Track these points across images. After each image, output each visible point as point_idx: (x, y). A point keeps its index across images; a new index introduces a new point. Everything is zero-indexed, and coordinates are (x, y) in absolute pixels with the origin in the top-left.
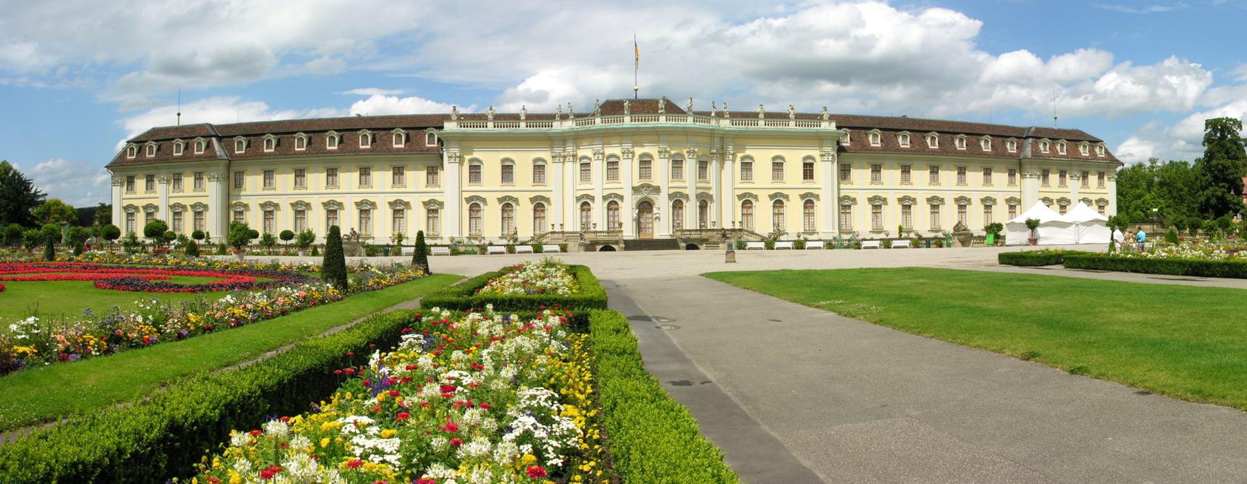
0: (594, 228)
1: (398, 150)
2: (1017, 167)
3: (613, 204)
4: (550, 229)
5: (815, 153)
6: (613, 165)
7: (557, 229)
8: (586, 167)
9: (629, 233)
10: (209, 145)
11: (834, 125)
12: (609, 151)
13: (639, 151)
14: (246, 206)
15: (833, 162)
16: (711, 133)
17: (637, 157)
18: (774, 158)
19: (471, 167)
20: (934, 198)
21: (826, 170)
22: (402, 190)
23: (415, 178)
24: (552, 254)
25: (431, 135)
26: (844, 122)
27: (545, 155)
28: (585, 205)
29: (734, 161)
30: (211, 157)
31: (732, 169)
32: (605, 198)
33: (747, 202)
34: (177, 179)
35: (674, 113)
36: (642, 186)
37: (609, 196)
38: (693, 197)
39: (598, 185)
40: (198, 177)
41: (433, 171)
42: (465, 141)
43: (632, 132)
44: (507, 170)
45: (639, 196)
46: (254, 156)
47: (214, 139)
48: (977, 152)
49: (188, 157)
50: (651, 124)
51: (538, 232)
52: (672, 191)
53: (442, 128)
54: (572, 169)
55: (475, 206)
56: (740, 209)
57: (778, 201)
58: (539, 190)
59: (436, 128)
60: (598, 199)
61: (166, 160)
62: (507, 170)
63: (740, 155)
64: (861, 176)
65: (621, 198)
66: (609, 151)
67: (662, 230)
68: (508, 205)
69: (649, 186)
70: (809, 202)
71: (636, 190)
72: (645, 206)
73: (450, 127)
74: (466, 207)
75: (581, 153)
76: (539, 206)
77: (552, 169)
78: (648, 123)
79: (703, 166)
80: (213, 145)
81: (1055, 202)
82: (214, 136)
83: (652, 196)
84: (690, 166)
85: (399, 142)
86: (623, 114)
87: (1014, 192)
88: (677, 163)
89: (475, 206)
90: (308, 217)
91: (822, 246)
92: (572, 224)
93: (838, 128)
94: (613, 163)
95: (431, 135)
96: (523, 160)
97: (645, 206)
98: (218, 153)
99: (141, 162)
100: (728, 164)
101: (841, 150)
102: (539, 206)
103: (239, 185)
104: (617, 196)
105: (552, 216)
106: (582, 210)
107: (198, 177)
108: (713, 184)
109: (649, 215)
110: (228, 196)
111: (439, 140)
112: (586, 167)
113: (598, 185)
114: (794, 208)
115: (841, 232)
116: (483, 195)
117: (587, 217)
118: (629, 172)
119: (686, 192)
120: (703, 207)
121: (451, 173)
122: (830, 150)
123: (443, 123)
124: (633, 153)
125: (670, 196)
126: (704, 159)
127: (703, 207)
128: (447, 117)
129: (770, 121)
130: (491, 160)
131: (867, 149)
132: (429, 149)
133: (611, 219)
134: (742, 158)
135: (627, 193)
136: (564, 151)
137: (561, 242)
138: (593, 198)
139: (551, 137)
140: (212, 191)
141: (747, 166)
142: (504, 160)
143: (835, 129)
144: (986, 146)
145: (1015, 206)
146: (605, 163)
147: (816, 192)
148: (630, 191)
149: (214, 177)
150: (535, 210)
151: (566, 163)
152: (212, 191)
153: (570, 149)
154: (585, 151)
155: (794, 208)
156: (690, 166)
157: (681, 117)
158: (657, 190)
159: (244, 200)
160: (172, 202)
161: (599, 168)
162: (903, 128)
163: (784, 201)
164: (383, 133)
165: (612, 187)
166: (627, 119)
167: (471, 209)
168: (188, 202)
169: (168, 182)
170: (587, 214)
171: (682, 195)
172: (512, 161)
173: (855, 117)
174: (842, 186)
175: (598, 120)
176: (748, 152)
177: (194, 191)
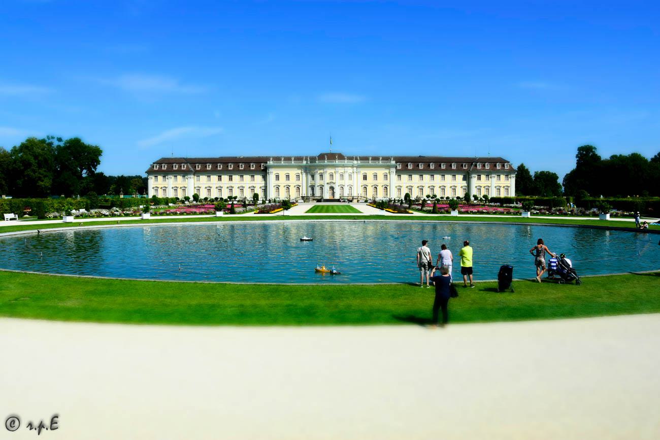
3: (322, 187)
6: (321, 176)
7: (303, 196)
8: (313, 177)
9: (327, 196)
10: (187, 167)
11: (394, 162)
21: (394, 176)
23: (259, 178)
26: (399, 160)
36: (331, 183)
44: (288, 177)
45: (329, 186)
50: (334, 163)
53: (267, 163)
61: (171, 171)
62: (288, 177)
64: (405, 177)
65: (323, 186)
67: (337, 197)
72: (332, 188)
73: (271, 163)
88: (342, 176)
93: (396, 162)
97: (332, 188)
112: (313, 177)
114: (380, 190)
116: (279, 184)
121: (271, 177)
130: (282, 173)
155: (380, 190)
156: (346, 176)
157: (343, 161)
158: (334, 183)
165: (322, 182)
168: (179, 186)
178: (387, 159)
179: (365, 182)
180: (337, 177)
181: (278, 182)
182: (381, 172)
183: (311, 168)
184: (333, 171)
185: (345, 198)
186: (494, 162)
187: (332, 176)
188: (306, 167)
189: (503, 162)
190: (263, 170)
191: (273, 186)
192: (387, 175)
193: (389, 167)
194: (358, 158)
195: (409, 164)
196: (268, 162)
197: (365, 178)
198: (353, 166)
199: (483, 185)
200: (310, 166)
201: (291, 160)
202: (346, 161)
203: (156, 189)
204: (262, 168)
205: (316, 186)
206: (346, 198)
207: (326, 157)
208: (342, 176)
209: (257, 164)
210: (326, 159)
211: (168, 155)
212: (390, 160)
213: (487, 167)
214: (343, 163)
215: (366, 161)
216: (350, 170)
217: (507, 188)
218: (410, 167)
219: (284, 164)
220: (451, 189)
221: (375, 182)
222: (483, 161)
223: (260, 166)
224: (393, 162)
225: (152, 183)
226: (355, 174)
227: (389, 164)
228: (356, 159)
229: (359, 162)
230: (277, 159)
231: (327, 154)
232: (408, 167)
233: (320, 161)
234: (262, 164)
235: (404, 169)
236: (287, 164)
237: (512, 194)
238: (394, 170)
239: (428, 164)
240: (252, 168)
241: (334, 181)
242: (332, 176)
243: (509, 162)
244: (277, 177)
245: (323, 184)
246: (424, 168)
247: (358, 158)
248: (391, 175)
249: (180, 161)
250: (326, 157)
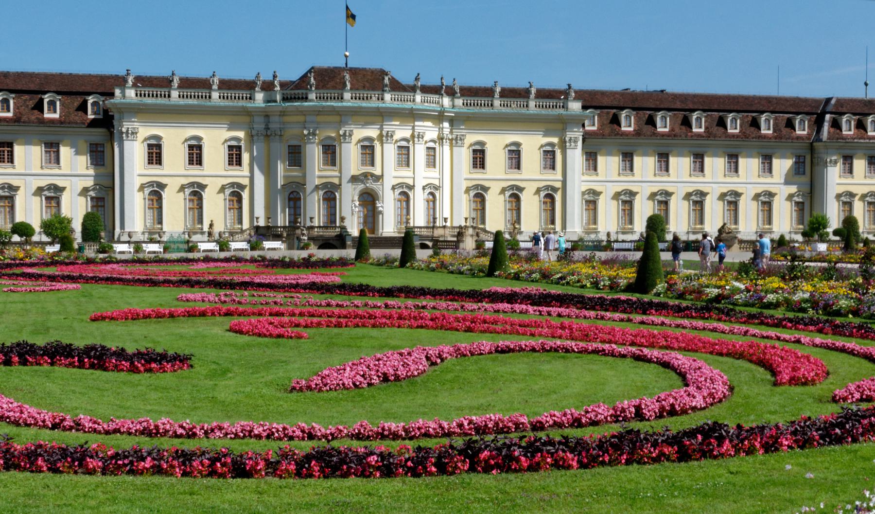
0: (311, 222)
1: (52, 121)
3: (330, 193)
24: (626, 253)
33: (479, 196)
35: (514, 97)
36: (366, 175)
43: (352, 111)
45: (361, 187)
48: (754, 136)
50: (374, 103)
53: (112, 95)
57: (515, 197)
59: (102, 94)
69: (372, 175)
72: (369, 200)
78: (470, 108)
90: (395, 211)
91: (736, 246)
106: (290, 199)
115: (588, 233)
120: (432, 200)
123: (114, 88)
127: (432, 200)
128: (120, 81)
129: (506, 101)
131: (618, 134)
139: (250, 112)
143: (581, 111)
157: (408, 95)
162: (662, 106)
166: (347, 95)
170: (295, 204)
173: (603, 93)
179: (479, 176)
180: (388, 154)
181: (155, 170)
183: (287, 119)
184: (372, 132)
187: (368, 150)
188: (267, 116)
190: (93, 124)
191: (137, 186)
192: (554, 152)
195: (623, 114)
196: (117, 92)
197: (479, 158)
198: (439, 117)
199: (860, 190)
200: (283, 113)
202: (418, 98)
204: (91, 116)
205: (309, 187)
207: (348, 77)
209: (68, 100)
210: (349, 86)
212: (566, 98)
214: (409, 105)
215: (483, 100)
216: (429, 131)
218: (628, 124)
219: (182, 102)
220: (754, 206)
223: (83, 108)
224: (575, 106)
226: (447, 148)
228: (451, 92)
229: (459, 102)
231: (354, 72)
232: (619, 125)
233: (325, 93)
234: (91, 100)
235: (607, 131)
236: (190, 102)
238: (577, 134)
239: (681, 114)
240: (47, 115)
241: (377, 171)
242: (368, 150)
245: (410, 182)
246: (672, 130)
248: (569, 152)
250: (348, 77)
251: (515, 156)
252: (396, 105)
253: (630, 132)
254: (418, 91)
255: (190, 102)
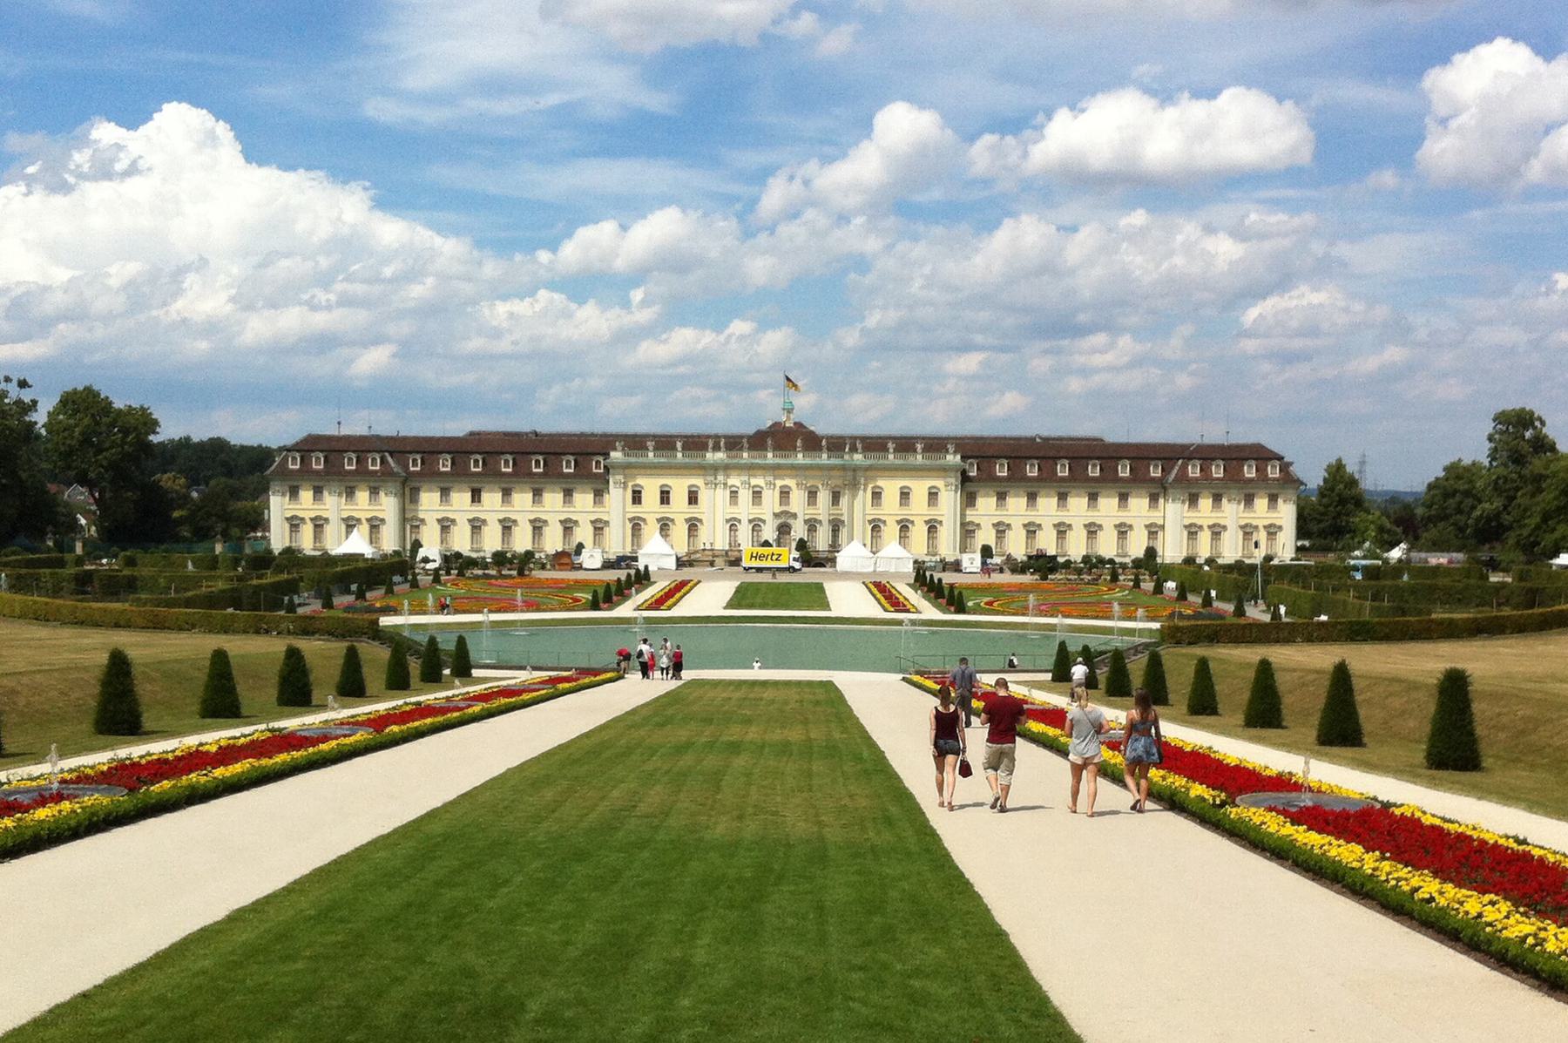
2: (1158, 491)
4: (702, 547)
5: (940, 483)
6: (757, 495)
7: (708, 547)
10: (383, 461)
11: (958, 457)
12: (754, 482)
13: (779, 483)
14: (423, 521)
15: (956, 492)
16: (843, 468)
17: (777, 489)
18: (901, 488)
19: (634, 492)
20: (1092, 524)
21: (949, 498)
22: (572, 509)
25: (598, 463)
27: (698, 482)
28: (733, 524)
29: (865, 490)
30: (386, 474)
31: (864, 497)
32: (750, 521)
34: (350, 493)
36: (782, 512)
37: (754, 520)
38: (826, 523)
39: (745, 509)
40: (374, 492)
41: (599, 494)
42: (625, 467)
44: (665, 497)
45: (780, 521)
46: (430, 475)
47: (387, 454)
49: (362, 473)
51: (691, 548)
52: (807, 517)
53: (606, 455)
54: (722, 495)
55: (637, 525)
56: (870, 532)
58: (693, 511)
60: (745, 522)
61: (339, 474)
62: (665, 497)
63: (870, 486)
64: (986, 506)
65: (764, 522)
66: (754, 482)
68: (666, 525)
70: (932, 527)
71: (776, 515)
73: (616, 455)
74: (629, 526)
75: (731, 482)
76: (693, 526)
77: (703, 496)
79: (836, 498)
80: (388, 462)
81: (1205, 528)
82: (387, 451)
83: (791, 521)
84: (824, 497)
85: (568, 466)
86: (766, 450)
87: (1155, 517)
89: (637, 525)
92: (721, 544)
94: (758, 492)
95: (598, 463)
96: (679, 486)
98: (395, 470)
99: (306, 472)
100: (861, 492)
101: (965, 478)
102: (693, 526)
103: (414, 500)
104: (760, 520)
105: (704, 538)
106: (731, 530)
107: (374, 492)
108: (845, 511)
109: (788, 537)
110: (403, 510)
111: (605, 467)
113: (745, 509)
117: (735, 536)
118: (771, 501)
119: (820, 518)
121: (617, 496)
122: (954, 480)
124: (774, 485)
125: (806, 522)
126: (837, 489)
130: (650, 486)
132: (596, 474)
133: (755, 539)
134: (873, 488)
135: (768, 517)
136: (716, 479)
137: (711, 558)
138: (740, 521)
140: (388, 506)
141: (877, 495)
142: (662, 486)
144: (1250, 472)
145: (1157, 532)
146: (751, 492)
147: (939, 518)
148: (771, 516)
149: (391, 492)
150: (690, 530)
151: (717, 490)
152: (388, 506)
153: (720, 478)
154: (734, 481)
157: (817, 453)
158: (795, 516)
159: (421, 515)
160: (345, 515)
161: (745, 496)
163: (910, 526)
164: (553, 457)
165: (756, 512)
166: (770, 455)
167: (633, 527)
169: (340, 495)
171: (815, 520)
172: (670, 487)
174: (968, 512)
175: (745, 455)
176: (880, 483)
177: (369, 505)
178: (935, 445)
182: (920, 488)
185: (821, 555)
186: (1235, 455)
189: (1261, 455)
193: (944, 470)
194: (859, 446)
196: (613, 454)
201: (674, 448)
203: (294, 523)
206: (826, 555)
208: (812, 495)
211: (331, 430)
213: (1217, 472)
217: (1273, 531)
219: (656, 460)
221: (904, 513)
222: (1206, 454)
224: (953, 459)
225: (278, 507)
227: (942, 461)
230: (635, 443)
233: (755, 453)
236: (662, 460)
237: (1285, 549)
240: (565, 471)
242: (785, 494)
243: (1281, 458)
244: (637, 497)
247: (859, 446)
249: (363, 446)
251: (905, 495)
252: (808, 461)
253: (1003, 477)
254: (825, 450)
255: (662, 460)
